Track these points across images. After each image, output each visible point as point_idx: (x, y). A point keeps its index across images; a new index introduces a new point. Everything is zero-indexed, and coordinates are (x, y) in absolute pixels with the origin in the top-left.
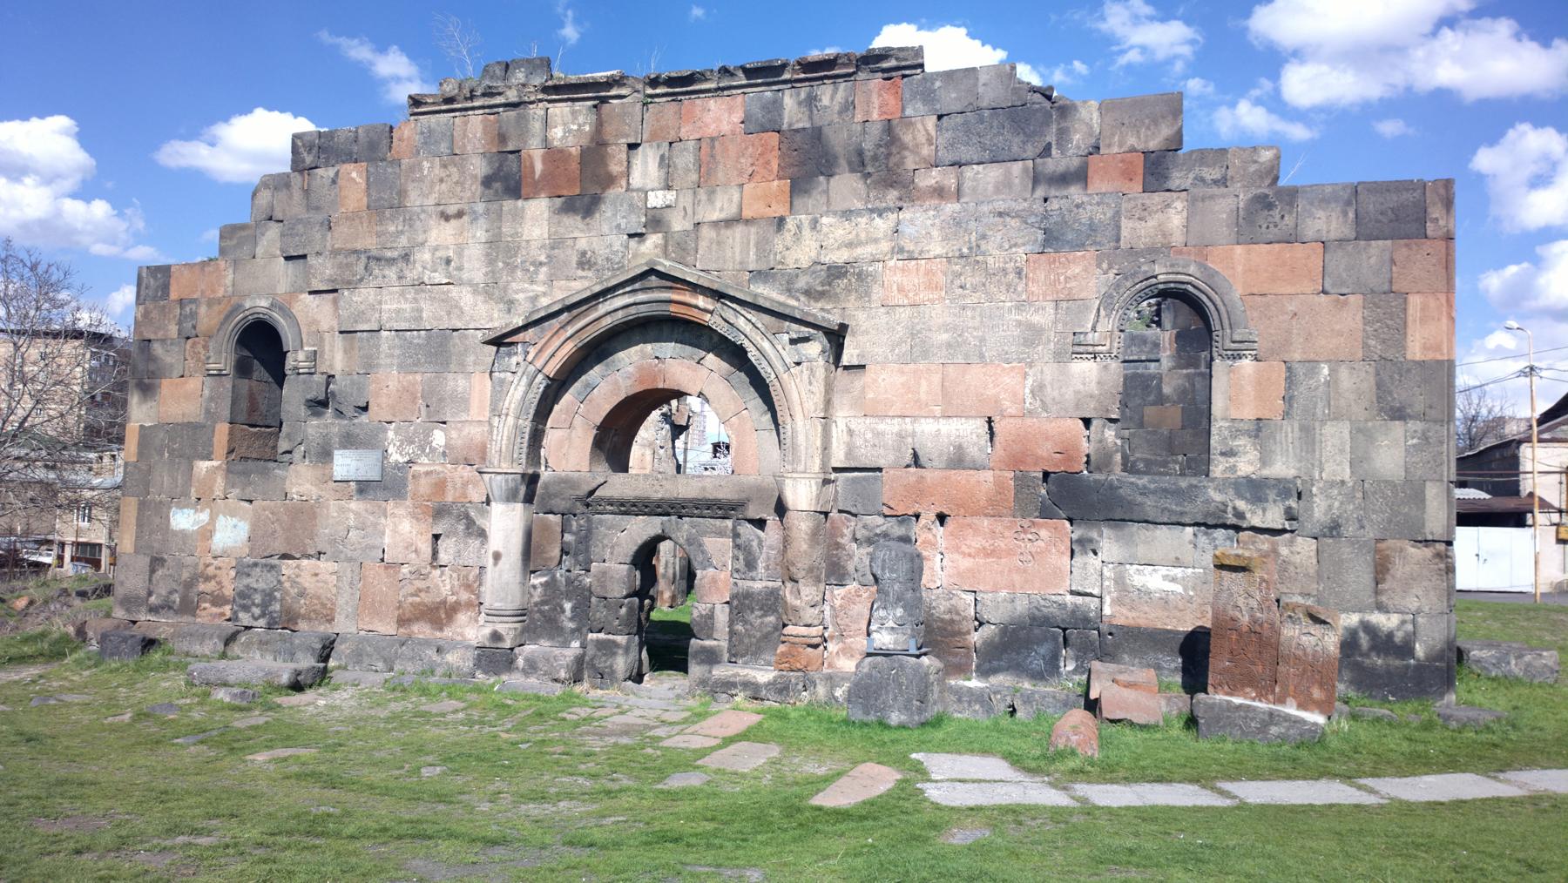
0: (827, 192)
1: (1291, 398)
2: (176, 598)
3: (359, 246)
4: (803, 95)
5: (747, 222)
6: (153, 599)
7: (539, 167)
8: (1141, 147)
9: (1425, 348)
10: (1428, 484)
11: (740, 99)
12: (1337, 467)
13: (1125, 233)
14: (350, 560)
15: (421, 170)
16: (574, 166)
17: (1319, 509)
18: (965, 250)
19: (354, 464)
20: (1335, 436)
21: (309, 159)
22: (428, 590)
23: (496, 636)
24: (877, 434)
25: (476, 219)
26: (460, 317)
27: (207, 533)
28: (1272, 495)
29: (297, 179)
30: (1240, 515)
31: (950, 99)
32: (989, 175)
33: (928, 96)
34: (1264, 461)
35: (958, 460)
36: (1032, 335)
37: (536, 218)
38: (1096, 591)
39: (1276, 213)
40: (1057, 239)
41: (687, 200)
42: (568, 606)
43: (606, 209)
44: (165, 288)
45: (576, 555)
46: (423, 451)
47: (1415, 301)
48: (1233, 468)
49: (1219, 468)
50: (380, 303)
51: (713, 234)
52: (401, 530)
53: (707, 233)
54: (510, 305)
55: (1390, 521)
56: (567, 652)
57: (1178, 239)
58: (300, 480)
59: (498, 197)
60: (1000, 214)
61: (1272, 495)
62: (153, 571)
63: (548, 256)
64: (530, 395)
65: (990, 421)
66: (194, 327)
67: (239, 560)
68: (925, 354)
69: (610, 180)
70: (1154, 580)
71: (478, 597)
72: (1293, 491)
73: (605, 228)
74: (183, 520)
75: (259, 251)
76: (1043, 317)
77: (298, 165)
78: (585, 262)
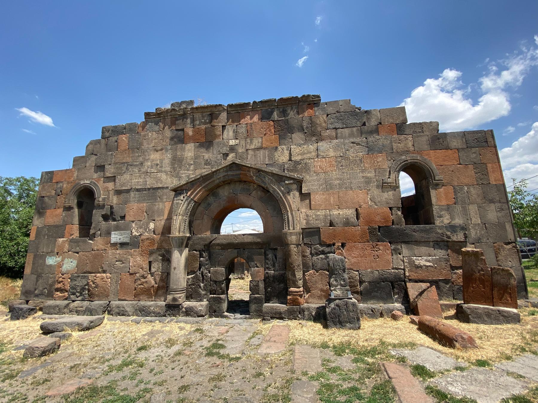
0: (291, 139)
1: (457, 197)
2: (46, 291)
3: (124, 161)
4: (281, 110)
5: (265, 148)
6: (36, 292)
7: (191, 133)
8: (395, 123)
9: (495, 180)
10: (506, 223)
11: (260, 111)
12: (476, 220)
13: (394, 147)
14: (116, 273)
15: (148, 135)
16: (203, 133)
17: (473, 234)
18: (342, 154)
19: (119, 237)
20: (473, 209)
21: (107, 134)
22: (146, 282)
23: (175, 299)
24: (317, 216)
25: (167, 150)
26: (161, 183)
27: (60, 265)
28: (459, 230)
29: (103, 141)
30: (449, 238)
31: (330, 110)
32: (347, 131)
33: (323, 109)
34: (452, 218)
35: (347, 223)
36: (368, 181)
37: (189, 151)
38: (402, 267)
39: (441, 140)
40: (372, 150)
41: (243, 142)
42: (202, 285)
43: (215, 146)
44: (51, 179)
45: (204, 266)
46: (146, 231)
47: (489, 166)
48: (442, 222)
49: (438, 222)
50: (131, 180)
51: (253, 153)
52: (137, 260)
53: (250, 152)
54: (180, 178)
55: (496, 236)
56: (202, 303)
57: (412, 149)
58: (98, 243)
59: (176, 143)
60: (352, 143)
61: (458, 229)
62: (37, 281)
63: (194, 162)
64: (189, 208)
65: (357, 210)
66: (61, 192)
67: (72, 274)
68: (331, 188)
69: (216, 136)
70: (422, 261)
71: (167, 284)
72: (463, 228)
73: (215, 152)
74: (51, 261)
75: (87, 165)
76: (371, 175)
77: (103, 137)
78: (207, 163)
